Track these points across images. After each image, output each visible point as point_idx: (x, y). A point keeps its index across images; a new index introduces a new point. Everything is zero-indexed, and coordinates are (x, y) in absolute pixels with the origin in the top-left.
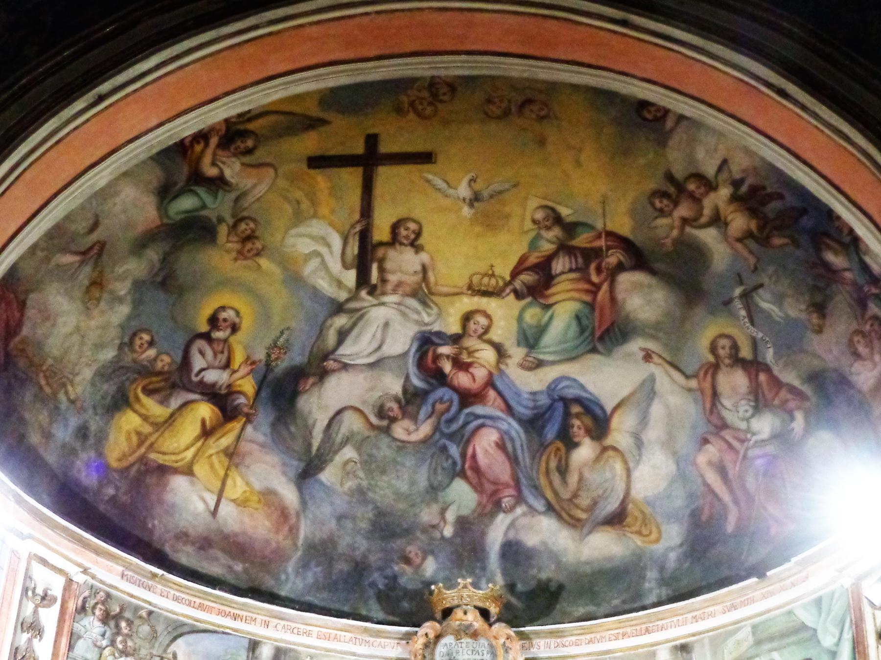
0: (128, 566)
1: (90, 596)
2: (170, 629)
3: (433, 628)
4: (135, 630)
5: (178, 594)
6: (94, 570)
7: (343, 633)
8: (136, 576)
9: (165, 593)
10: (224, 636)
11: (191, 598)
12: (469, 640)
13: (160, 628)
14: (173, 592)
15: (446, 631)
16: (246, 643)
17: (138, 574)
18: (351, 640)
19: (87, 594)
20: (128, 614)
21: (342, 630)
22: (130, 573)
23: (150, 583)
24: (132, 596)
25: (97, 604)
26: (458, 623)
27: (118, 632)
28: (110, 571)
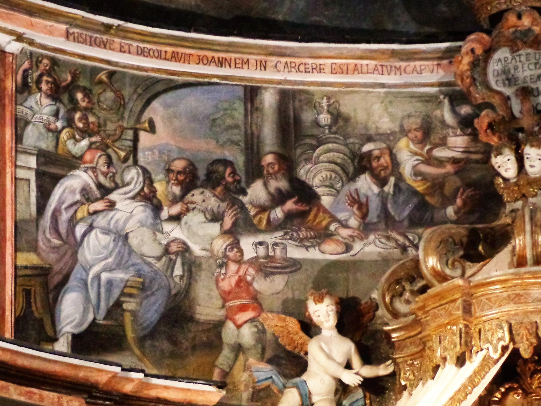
0: (71, 21)
1: (31, 68)
2: (140, 91)
3: (479, 42)
4: (95, 100)
5: (142, 45)
6: (29, 33)
7: (365, 62)
8: (85, 32)
9: (126, 47)
10: (212, 88)
11: (160, 48)
12: (529, 51)
13: (127, 92)
14: (135, 44)
15: (498, 42)
16: (240, 92)
17: (87, 29)
18: (375, 69)
19: (26, 65)
20: (83, 82)
21: (361, 58)
22: (76, 30)
23: (104, 37)
24: (84, 57)
25: (41, 76)
26: (511, 30)
27: (74, 106)
28: (51, 33)
